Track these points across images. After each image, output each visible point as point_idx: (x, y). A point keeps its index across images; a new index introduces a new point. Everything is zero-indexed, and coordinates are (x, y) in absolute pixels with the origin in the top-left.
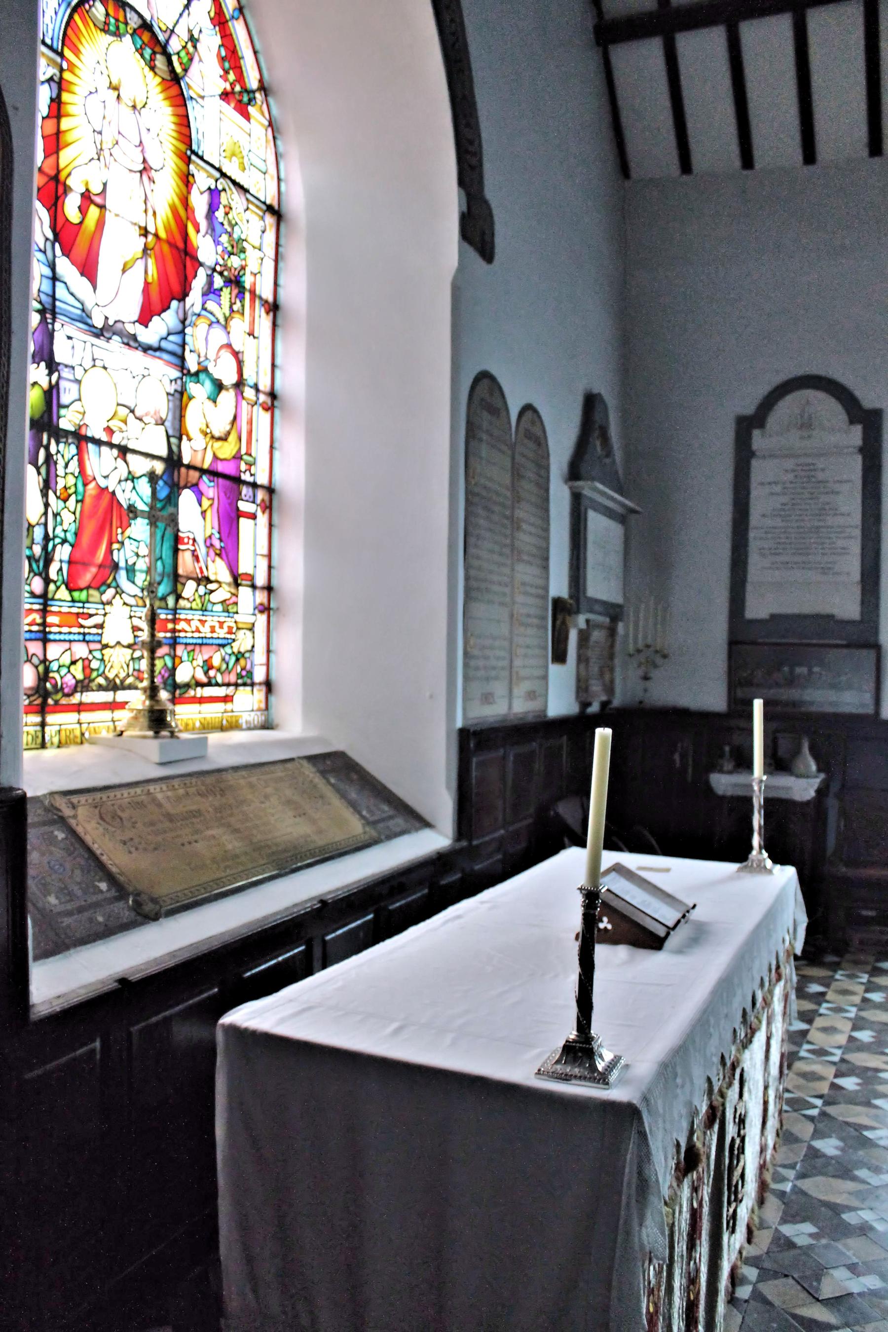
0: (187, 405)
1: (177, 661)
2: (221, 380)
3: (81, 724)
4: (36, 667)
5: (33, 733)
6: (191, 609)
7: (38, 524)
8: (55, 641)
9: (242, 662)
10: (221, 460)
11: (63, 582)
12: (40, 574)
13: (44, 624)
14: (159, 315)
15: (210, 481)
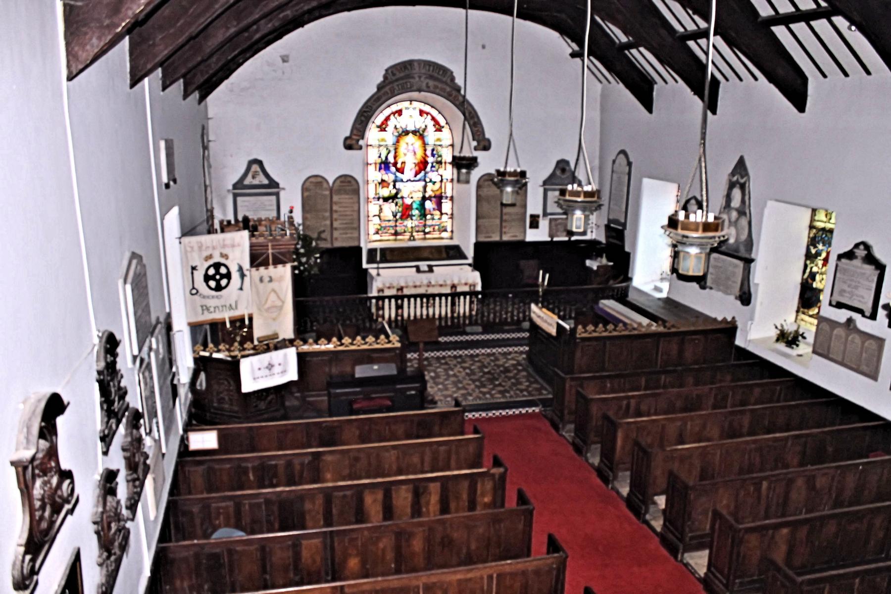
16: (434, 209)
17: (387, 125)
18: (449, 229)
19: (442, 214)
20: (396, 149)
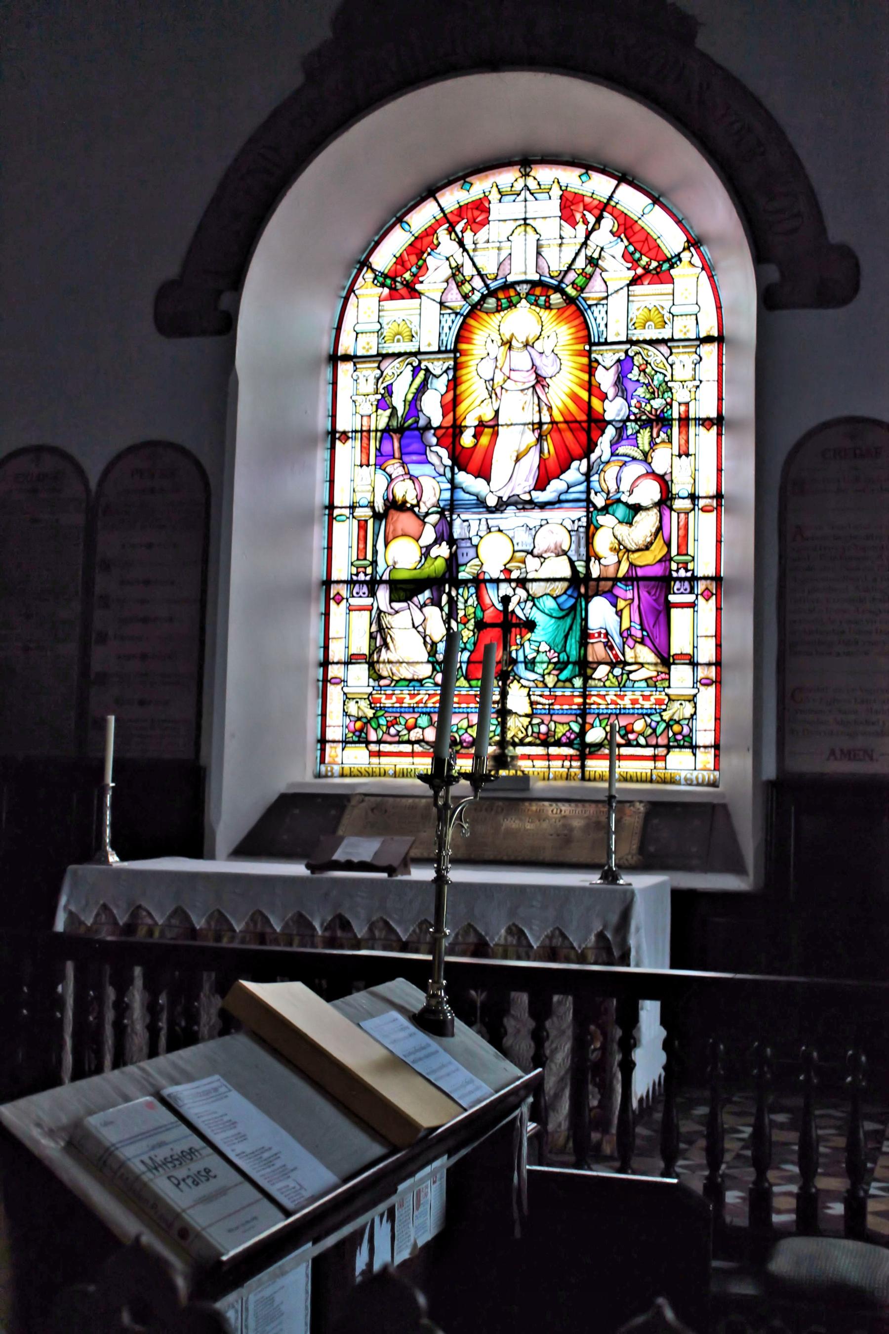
0: (594, 535)
1: (587, 726)
2: (639, 504)
6: (605, 686)
7: (441, 641)
9: (676, 728)
10: (641, 567)
11: (463, 675)
14: (558, 478)
15: (627, 585)
17: (423, 268)
19: (666, 660)
20: (457, 367)
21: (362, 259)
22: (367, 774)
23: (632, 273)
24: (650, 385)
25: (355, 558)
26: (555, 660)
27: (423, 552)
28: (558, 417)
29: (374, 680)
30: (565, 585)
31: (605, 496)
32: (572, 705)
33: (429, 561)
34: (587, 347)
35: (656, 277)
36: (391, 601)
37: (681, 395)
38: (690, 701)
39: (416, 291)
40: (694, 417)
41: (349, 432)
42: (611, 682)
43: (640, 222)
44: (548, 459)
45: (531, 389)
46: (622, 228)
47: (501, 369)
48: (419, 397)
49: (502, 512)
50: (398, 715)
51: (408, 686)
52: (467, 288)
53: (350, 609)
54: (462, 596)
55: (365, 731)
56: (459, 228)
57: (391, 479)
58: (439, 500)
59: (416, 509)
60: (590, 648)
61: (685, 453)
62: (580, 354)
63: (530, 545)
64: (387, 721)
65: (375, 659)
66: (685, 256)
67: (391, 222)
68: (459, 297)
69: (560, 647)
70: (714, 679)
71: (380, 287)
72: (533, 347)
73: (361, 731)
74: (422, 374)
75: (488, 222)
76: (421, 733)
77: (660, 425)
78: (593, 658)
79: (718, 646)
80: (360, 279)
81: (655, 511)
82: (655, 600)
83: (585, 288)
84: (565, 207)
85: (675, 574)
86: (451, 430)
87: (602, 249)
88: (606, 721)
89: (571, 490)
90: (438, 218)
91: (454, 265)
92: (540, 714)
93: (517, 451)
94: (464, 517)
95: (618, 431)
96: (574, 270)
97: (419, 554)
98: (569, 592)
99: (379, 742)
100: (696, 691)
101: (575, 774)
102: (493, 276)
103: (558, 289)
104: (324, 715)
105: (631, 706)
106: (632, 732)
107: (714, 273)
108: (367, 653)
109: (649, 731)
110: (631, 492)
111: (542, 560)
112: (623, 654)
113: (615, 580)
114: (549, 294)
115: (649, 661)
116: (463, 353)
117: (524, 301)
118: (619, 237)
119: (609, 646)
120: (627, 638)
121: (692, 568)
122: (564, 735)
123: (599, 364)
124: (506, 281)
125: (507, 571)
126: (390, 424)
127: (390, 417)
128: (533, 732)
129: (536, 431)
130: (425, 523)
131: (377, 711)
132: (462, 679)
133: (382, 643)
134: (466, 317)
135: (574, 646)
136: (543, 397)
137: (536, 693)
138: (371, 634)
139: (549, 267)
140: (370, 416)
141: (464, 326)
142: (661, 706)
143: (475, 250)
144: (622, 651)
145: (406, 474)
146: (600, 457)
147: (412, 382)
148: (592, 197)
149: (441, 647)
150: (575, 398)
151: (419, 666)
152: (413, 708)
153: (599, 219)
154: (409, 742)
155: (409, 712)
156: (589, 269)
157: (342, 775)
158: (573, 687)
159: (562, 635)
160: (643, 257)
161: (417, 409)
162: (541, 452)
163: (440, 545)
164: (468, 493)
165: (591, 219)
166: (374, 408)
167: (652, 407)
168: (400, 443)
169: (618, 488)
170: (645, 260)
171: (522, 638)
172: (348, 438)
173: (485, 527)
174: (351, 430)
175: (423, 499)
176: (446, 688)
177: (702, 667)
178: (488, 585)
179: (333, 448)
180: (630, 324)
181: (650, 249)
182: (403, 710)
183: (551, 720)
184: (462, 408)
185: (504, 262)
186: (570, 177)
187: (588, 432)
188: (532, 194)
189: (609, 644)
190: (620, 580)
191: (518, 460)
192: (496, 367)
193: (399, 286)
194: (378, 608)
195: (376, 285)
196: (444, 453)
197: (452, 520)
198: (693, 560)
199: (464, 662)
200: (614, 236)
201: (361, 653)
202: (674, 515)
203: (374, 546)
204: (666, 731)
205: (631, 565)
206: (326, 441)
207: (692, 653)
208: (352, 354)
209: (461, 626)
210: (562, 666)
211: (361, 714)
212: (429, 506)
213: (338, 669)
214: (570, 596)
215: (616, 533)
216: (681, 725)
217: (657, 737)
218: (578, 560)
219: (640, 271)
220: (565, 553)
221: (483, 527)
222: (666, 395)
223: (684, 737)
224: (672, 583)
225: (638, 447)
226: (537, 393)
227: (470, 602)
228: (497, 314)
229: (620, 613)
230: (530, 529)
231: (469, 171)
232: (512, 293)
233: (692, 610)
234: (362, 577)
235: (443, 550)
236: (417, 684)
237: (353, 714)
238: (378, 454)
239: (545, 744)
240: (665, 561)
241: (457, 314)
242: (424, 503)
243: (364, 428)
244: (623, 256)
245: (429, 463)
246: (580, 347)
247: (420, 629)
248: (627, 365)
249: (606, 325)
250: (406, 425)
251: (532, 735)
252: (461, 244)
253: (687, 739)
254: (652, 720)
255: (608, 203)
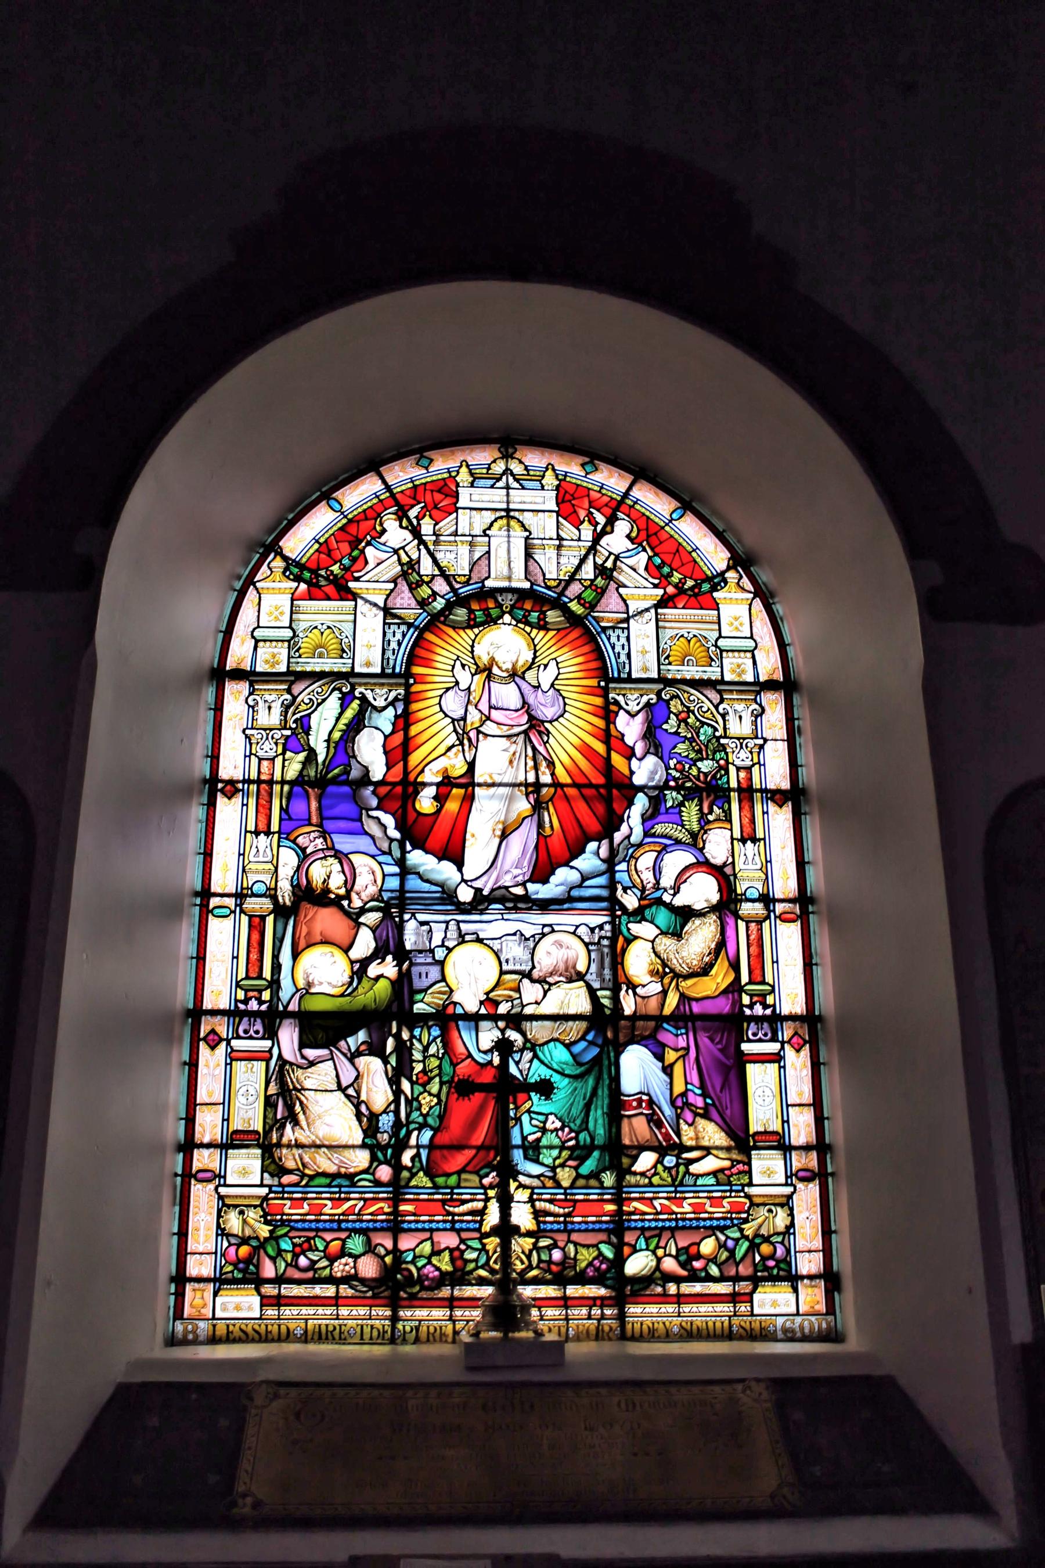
0: (624, 951)
1: (626, 1250)
2: (689, 907)
3: (454, 1322)
4: (382, 1258)
5: (381, 1328)
6: (651, 1185)
7: (385, 1112)
8: (410, 1230)
9: (766, 1249)
10: (697, 1000)
11: (421, 1169)
12: (387, 1162)
13: (396, 1212)
14: (566, 864)
15: (677, 1028)
16: (680, 1103)
18: (808, 1264)
20: (409, 699)
21: (267, 543)
22: (257, 1337)
23: (661, 592)
24: (695, 741)
25: (242, 974)
26: (572, 1143)
27: (355, 969)
28: (563, 777)
29: (272, 1175)
30: (584, 1025)
31: (639, 894)
32: (602, 1216)
33: (365, 983)
34: (603, 684)
35: (693, 598)
36: (302, 1045)
37: (741, 757)
38: (782, 1205)
39: (349, 590)
40: (758, 787)
41: (238, 782)
42: (661, 1179)
43: (667, 528)
44: (550, 835)
45: (522, 736)
46: (643, 534)
47: (476, 706)
48: (350, 738)
49: (482, 912)
50: (312, 1234)
51: (329, 1186)
52: (425, 591)
53: (233, 1056)
54: (420, 1041)
55: (255, 1261)
56: (413, 513)
57: (304, 856)
58: (381, 890)
59: (345, 903)
60: (625, 1123)
61: (749, 837)
62: (591, 691)
63: (527, 962)
64: (294, 1245)
65: (275, 1141)
66: (731, 575)
67: (314, 497)
68: (413, 603)
69: (578, 1122)
70: (817, 1170)
71: (293, 580)
72: (523, 678)
73: (248, 1261)
74: (355, 705)
75: (456, 510)
76: (352, 1264)
77: (712, 797)
78: (631, 1140)
79: (819, 1120)
80: (265, 567)
81: (713, 917)
82: (719, 1050)
83: (596, 605)
84: (563, 501)
85: (748, 1012)
86: (399, 789)
87: (617, 558)
88: (656, 1240)
89: (587, 883)
90: (382, 497)
91: (405, 559)
92: (551, 1231)
93: (503, 823)
94: (421, 917)
95: (653, 801)
96: (580, 580)
97: (348, 972)
98: (590, 1037)
99: (279, 1280)
100: (789, 1190)
101: (611, 1329)
102: (463, 579)
103: (558, 604)
104: (183, 1234)
105: (692, 1216)
106: (698, 1256)
107: (771, 601)
108: (261, 1130)
109: (725, 1255)
110: (676, 890)
111: (546, 987)
112: (678, 1135)
113: (660, 1019)
114: (544, 609)
115: (718, 1143)
116: (420, 679)
117: (507, 618)
118: (640, 544)
119: (655, 1121)
120: (682, 1109)
121: (772, 1003)
122: (590, 1264)
123: (621, 707)
124: (484, 586)
125: (489, 1001)
126: (305, 773)
127: (305, 764)
128: (540, 1261)
129: (531, 796)
130: (359, 925)
131: (276, 1227)
132: (421, 1174)
133: (286, 1114)
134: (422, 631)
135: (600, 1121)
136: (541, 749)
137: (544, 1197)
138: (267, 1098)
139: (544, 575)
140: (272, 760)
141: (418, 643)
142: (738, 1218)
143: (436, 543)
144: (675, 1128)
145: (328, 849)
146: (628, 837)
147: (341, 714)
148: (600, 492)
149: (386, 1121)
150: (586, 750)
151: (349, 1154)
152: (339, 1222)
153: (611, 520)
154: (331, 1280)
155: (332, 1230)
156: (600, 583)
157: (213, 1340)
158: (602, 1187)
159: (582, 1103)
160: (675, 573)
161: (347, 754)
162: (540, 825)
163: (383, 960)
164: (427, 881)
165: (601, 519)
166: (280, 750)
167: (699, 769)
168: (319, 802)
169: (658, 882)
170: (676, 577)
171: (517, 1108)
172: (237, 790)
173: (455, 935)
174: (241, 778)
175: (357, 888)
176: (397, 1189)
177: (798, 1152)
178: (460, 1023)
179: (211, 805)
180: (662, 656)
181: (683, 565)
182: (320, 1225)
183: (569, 1241)
184: (415, 758)
185: (480, 562)
186: (572, 467)
187: (608, 801)
188: (516, 480)
189: (655, 1117)
190: (668, 1019)
191: (504, 836)
192: (469, 702)
193: (323, 583)
194: (280, 1056)
195: (288, 577)
196: (388, 820)
197: (402, 921)
198: (773, 991)
199: (423, 1147)
200: (633, 543)
201: (251, 1129)
202: (742, 925)
203: (276, 957)
204: (750, 1254)
205: (683, 998)
206: (201, 793)
207: (780, 1131)
208: (249, 669)
209: (418, 1089)
210: (584, 1153)
211: (248, 1232)
212: (366, 899)
213: (209, 1156)
214: (591, 1043)
215: (660, 949)
216: (772, 1244)
217: (737, 1264)
218: (601, 989)
219: (670, 590)
220: (580, 977)
221: (453, 934)
222: (718, 756)
223: (778, 1262)
224: (745, 1025)
225: (683, 826)
226: (531, 742)
227: (433, 1050)
228: (468, 631)
229: (669, 1070)
230: (527, 939)
231: (429, 443)
232: (491, 604)
233: (776, 1065)
234: (254, 1005)
235: (389, 968)
236: (346, 1183)
237: (235, 1232)
238: (284, 816)
239: (560, 1280)
240: (733, 992)
241: (410, 625)
242: (358, 894)
243: (263, 777)
244: (646, 569)
245: (366, 833)
246: (593, 682)
247: (351, 1091)
248: (660, 711)
249: (629, 656)
250: (330, 776)
251: (538, 1267)
252: (416, 533)
253: (782, 1266)
254: (728, 1237)
255: (622, 502)
